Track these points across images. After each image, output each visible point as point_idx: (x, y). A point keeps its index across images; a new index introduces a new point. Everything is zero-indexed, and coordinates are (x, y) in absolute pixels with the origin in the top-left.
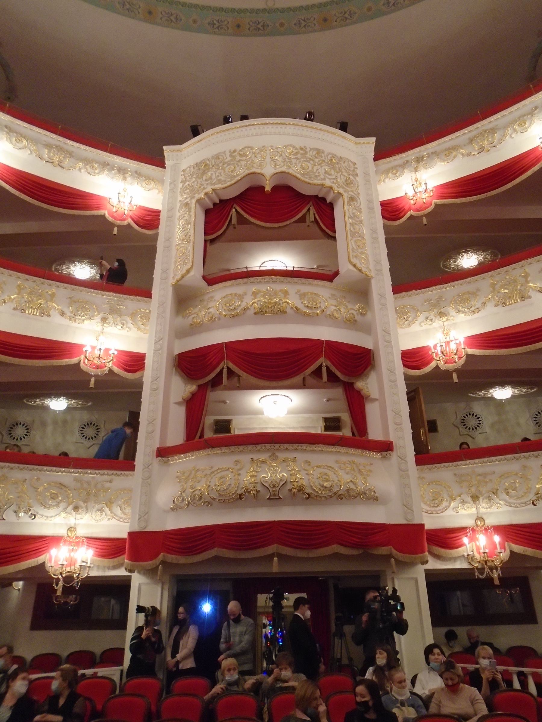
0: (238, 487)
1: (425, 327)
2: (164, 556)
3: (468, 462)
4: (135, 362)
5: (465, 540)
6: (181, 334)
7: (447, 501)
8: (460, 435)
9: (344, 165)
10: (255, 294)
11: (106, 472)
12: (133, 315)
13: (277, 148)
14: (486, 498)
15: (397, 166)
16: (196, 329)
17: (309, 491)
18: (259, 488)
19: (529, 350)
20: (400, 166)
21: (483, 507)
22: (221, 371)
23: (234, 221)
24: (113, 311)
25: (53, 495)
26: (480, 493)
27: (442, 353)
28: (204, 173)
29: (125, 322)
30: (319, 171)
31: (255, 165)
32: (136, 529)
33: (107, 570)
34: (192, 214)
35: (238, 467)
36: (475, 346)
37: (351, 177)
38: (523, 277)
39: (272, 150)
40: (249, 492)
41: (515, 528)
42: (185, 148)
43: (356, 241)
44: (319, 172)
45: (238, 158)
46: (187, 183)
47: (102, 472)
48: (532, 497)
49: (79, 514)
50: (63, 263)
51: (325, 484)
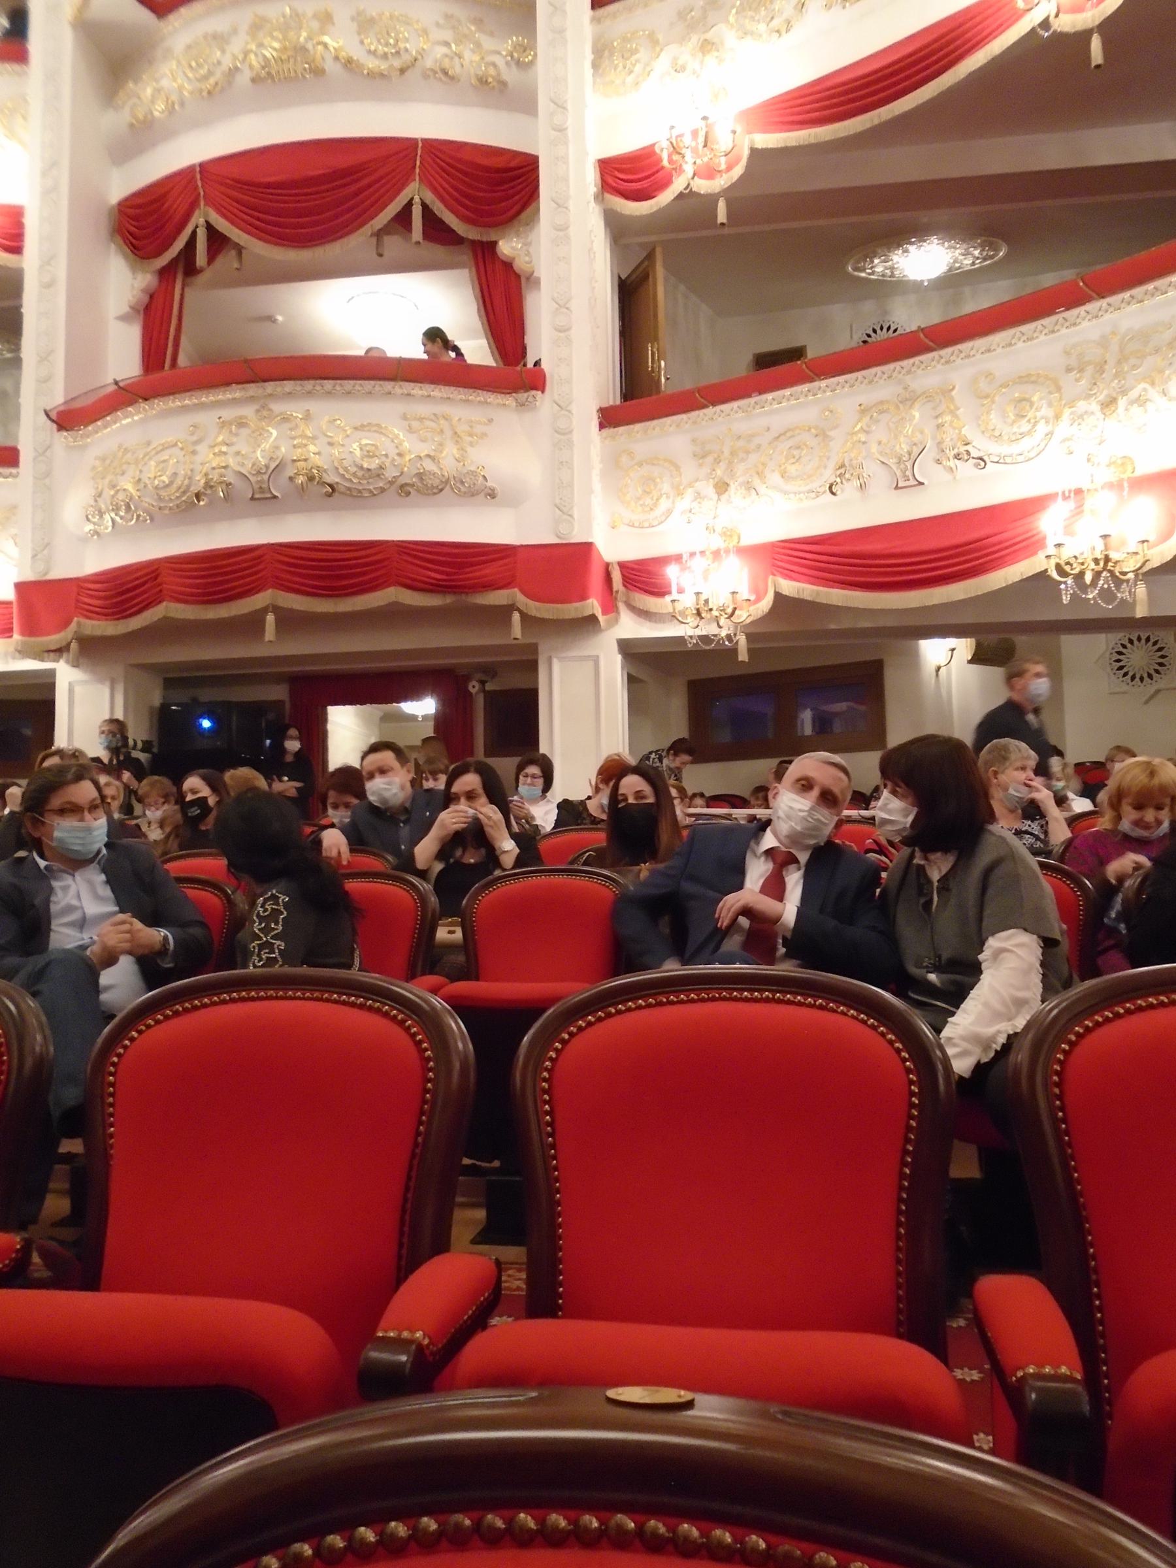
2: (79, 624)
14: (741, 485)
17: (332, 478)
18: (230, 478)
19: (876, 122)
22: (194, 233)
32: (29, 576)
33: (10, 660)
35: (195, 438)
36: (776, 123)
41: (787, 545)
48: (829, 475)
51: (365, 466)
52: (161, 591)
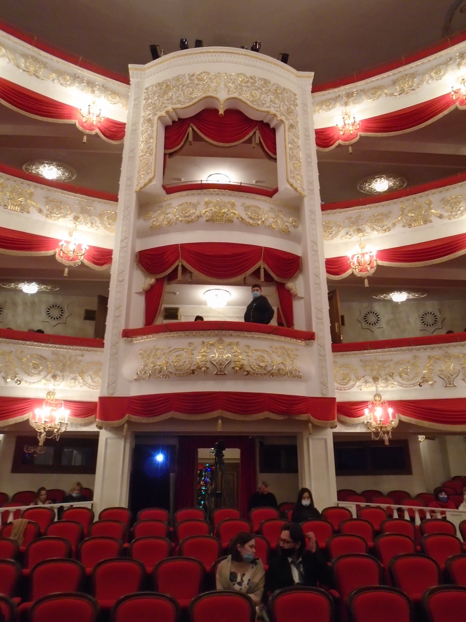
0: (191, 364)
1: (345, 240)
2: (129, 417)
3: (372, 351)
4: (103, 257)
5: (366, 411)
6: (141, 234)
7: (353, 380)
8: (362, 329)
9: (286, 95)
10: (207, 204)
11: (78, 347)
12: (101, 216)
13: (231, 75)
15: (330, 99)
16: (155, 230)
18: (209, 365)
19: (426, 265)
20: (333, 99)
21: (381, 386)
22: (176, 269)
23: (191, 138)
24: (84, 211)
25: (35, 365)
26: (380, 375)
27: (359, 263)
28: (165, 93)
29: (94, 221)
30: (265, 99)
31: (211, 90)
32: (106, 394)
34: (155, 129)
35: (191, 348)
37: (292, 107)
38: (427, 204)
39: (226, 77)
40: (200, 368)
41: (405, 403)
42: (148, 68)
43: (293, 164)
44: (265, 101)
45: (196, 82)
46: (150, 101)
47: (75, 347)
48: (419, 380)
49: (57, 381)
50: (34, 164)
51: (262, 364)
52: (171, 407)
